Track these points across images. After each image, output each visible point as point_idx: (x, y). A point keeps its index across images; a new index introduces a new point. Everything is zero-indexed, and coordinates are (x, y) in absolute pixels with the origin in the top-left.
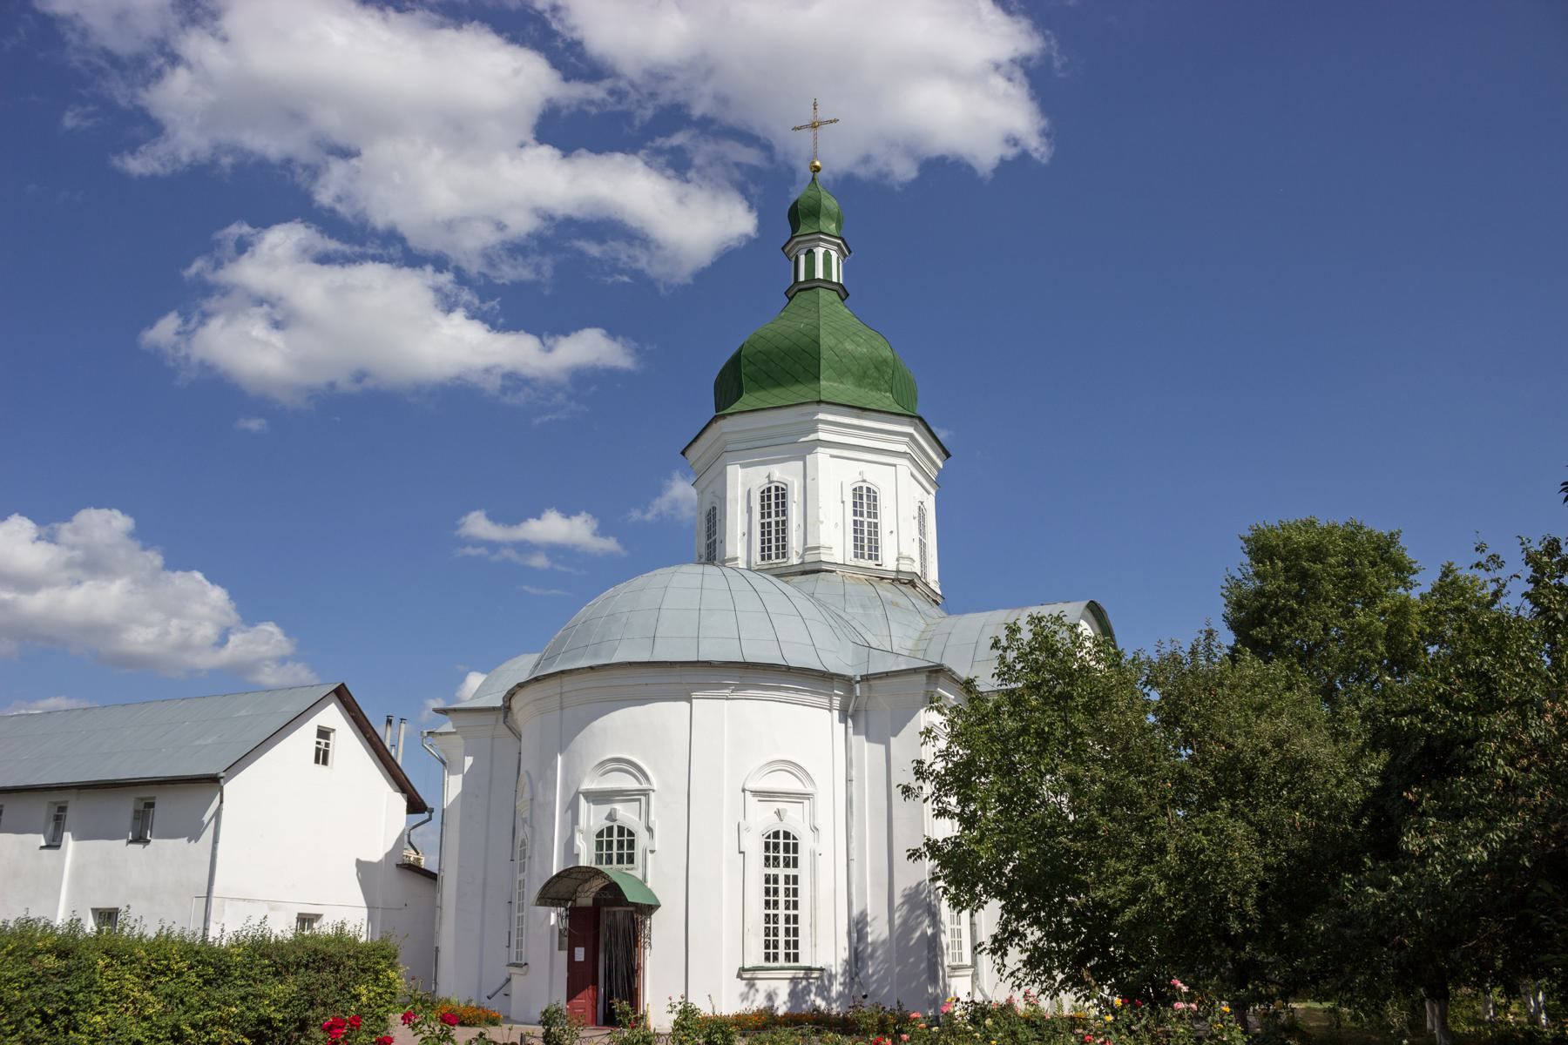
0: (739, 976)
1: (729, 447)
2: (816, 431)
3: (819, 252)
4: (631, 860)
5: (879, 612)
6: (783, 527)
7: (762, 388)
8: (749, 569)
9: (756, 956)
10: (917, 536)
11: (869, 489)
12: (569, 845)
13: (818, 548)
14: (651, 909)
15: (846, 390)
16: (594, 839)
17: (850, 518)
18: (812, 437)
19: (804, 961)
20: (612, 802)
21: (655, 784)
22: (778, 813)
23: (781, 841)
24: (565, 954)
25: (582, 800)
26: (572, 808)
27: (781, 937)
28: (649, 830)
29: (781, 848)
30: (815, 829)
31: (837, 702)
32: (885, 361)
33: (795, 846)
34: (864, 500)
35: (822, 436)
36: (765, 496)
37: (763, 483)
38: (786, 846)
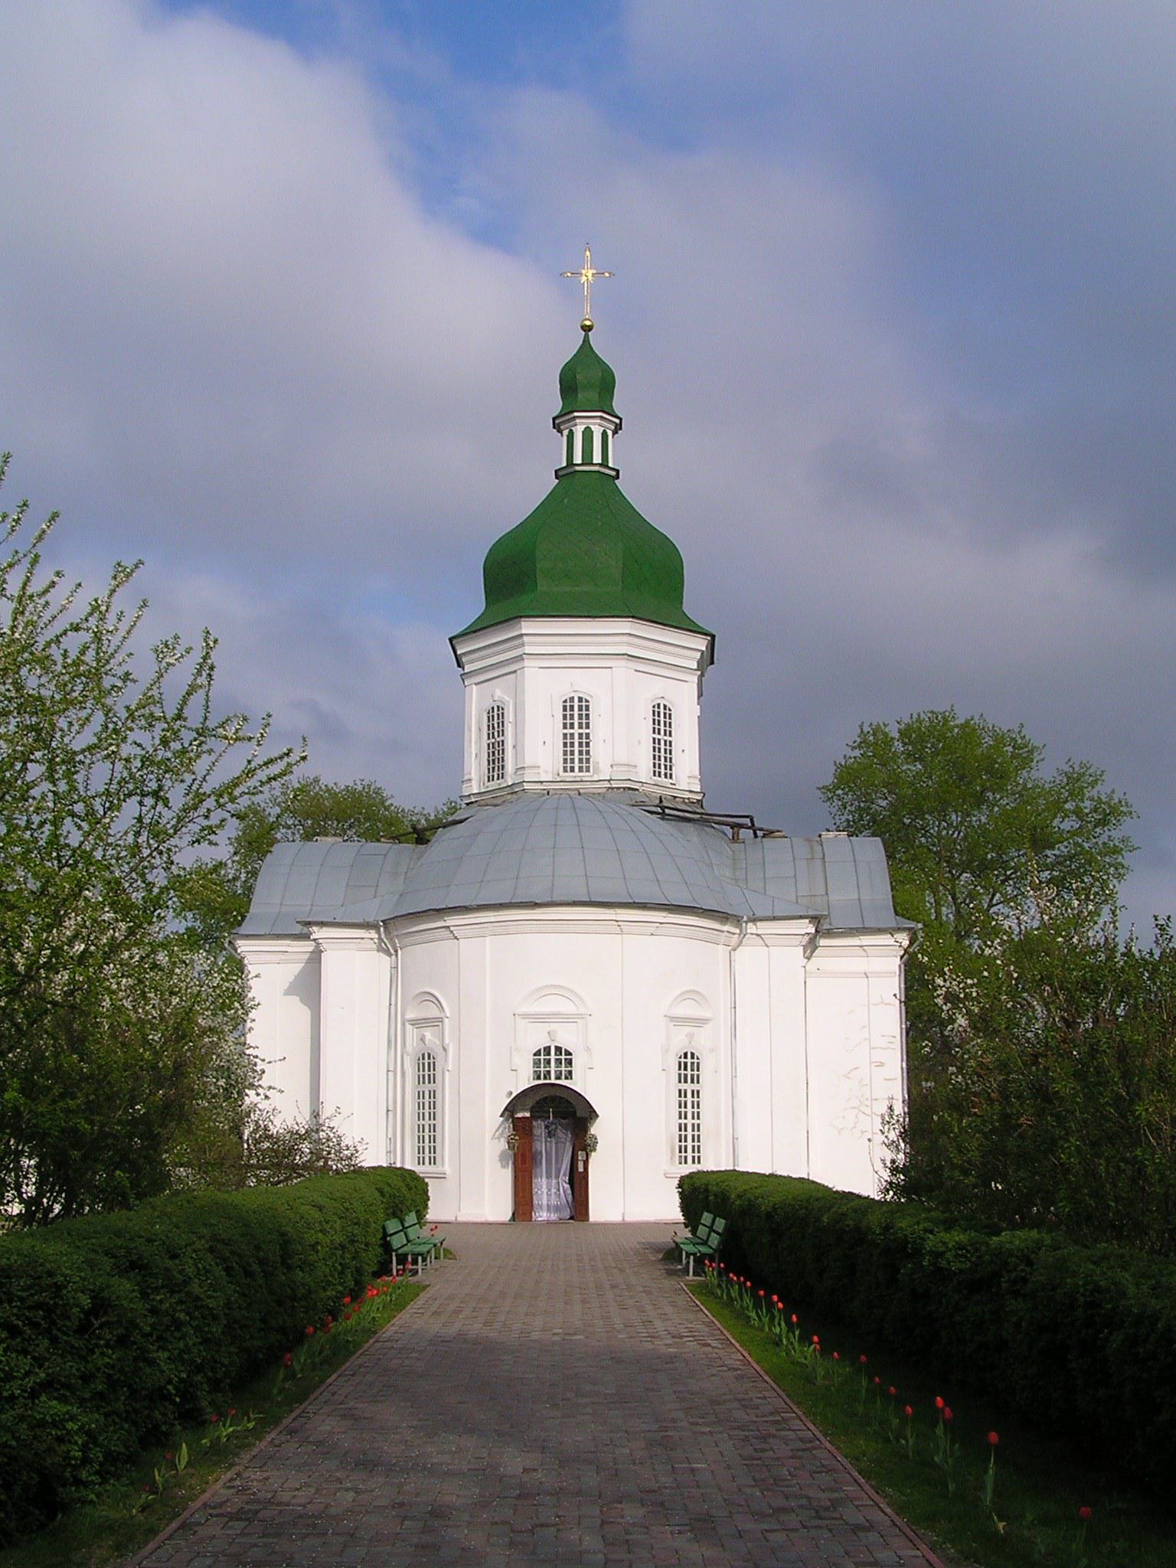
6: (586, 742)
23: (689, 1060)
28: (588, 1049)
29: (688, 1066)
36: (567, 707)
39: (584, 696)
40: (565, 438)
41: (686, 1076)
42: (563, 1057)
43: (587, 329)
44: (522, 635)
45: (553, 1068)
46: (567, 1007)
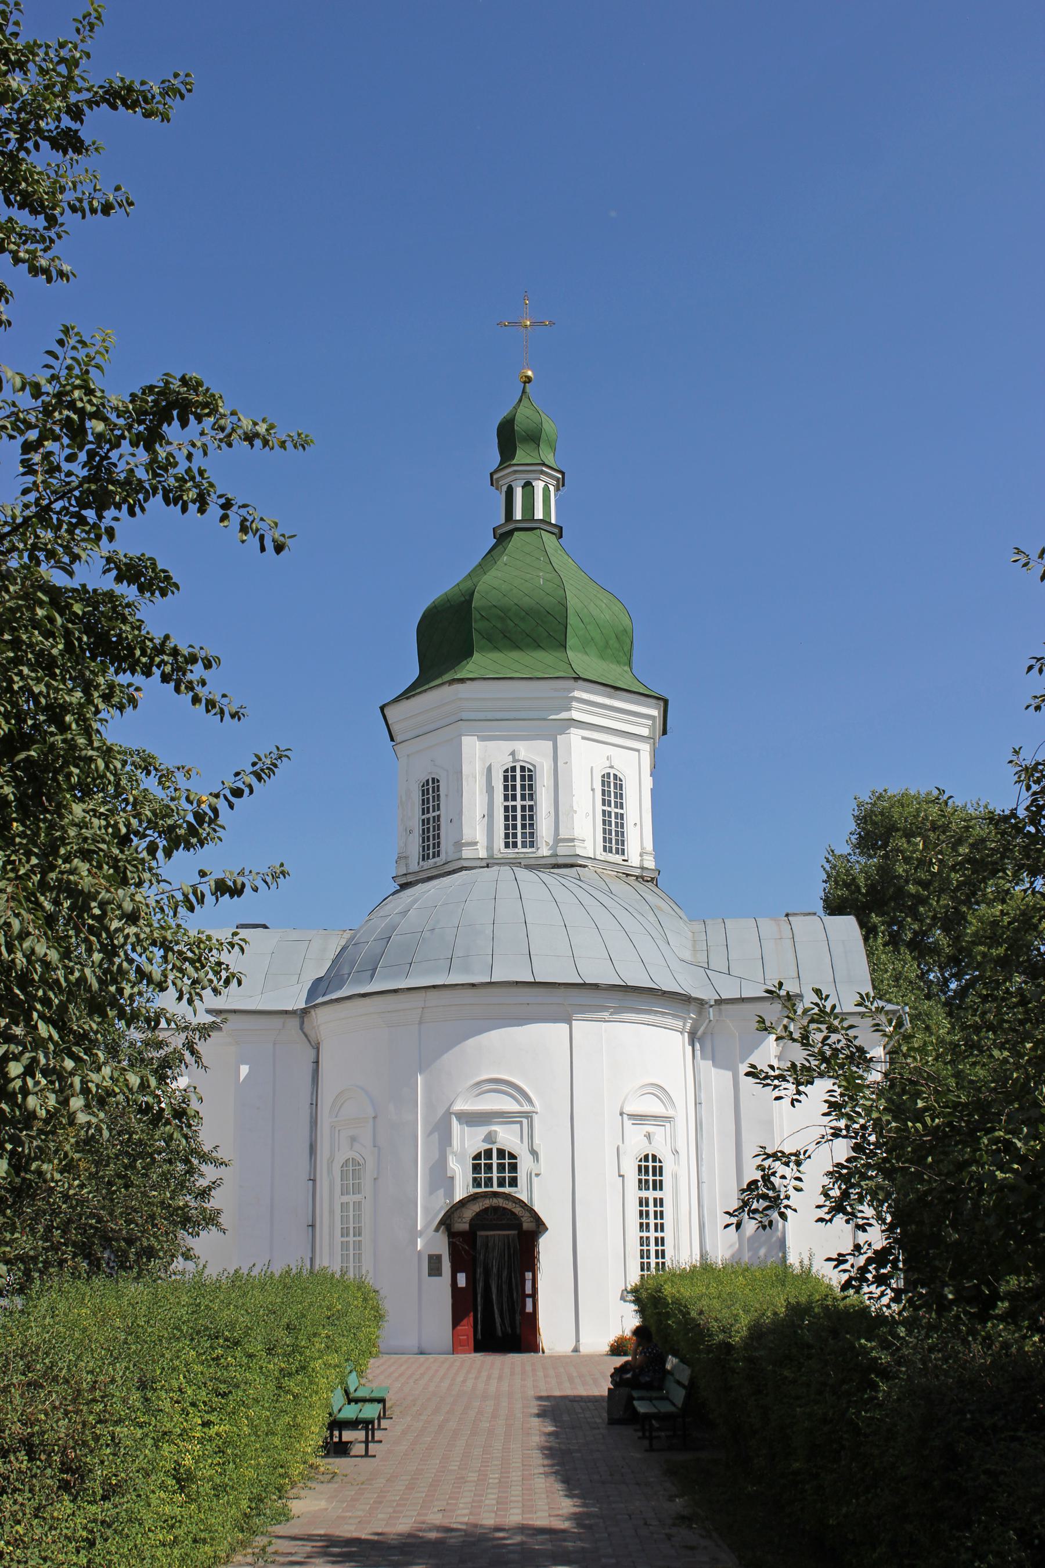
0: (623, 1298)
2: (569, 709)
3: (539, 486)
4: (514, 1182)
6: (530, 814)
7: (497, 648)
11: (615, 776)
13: (573, 840)
17: (599, 807)
18: (564, 715)
21: (538, 1106)
22: (648, 1136)
23: (650, 1164)
25: (455, 1121)
28: (534, 1153)
29: (651, 1171)
35: (575, 715)
36: (509, 776)
39: (527, 766)
40: (504, 494)
41: (647, 1181)
42: (507, 1161)
44: (461, 699)
45: (495, 1175)
46: (509, 1105)
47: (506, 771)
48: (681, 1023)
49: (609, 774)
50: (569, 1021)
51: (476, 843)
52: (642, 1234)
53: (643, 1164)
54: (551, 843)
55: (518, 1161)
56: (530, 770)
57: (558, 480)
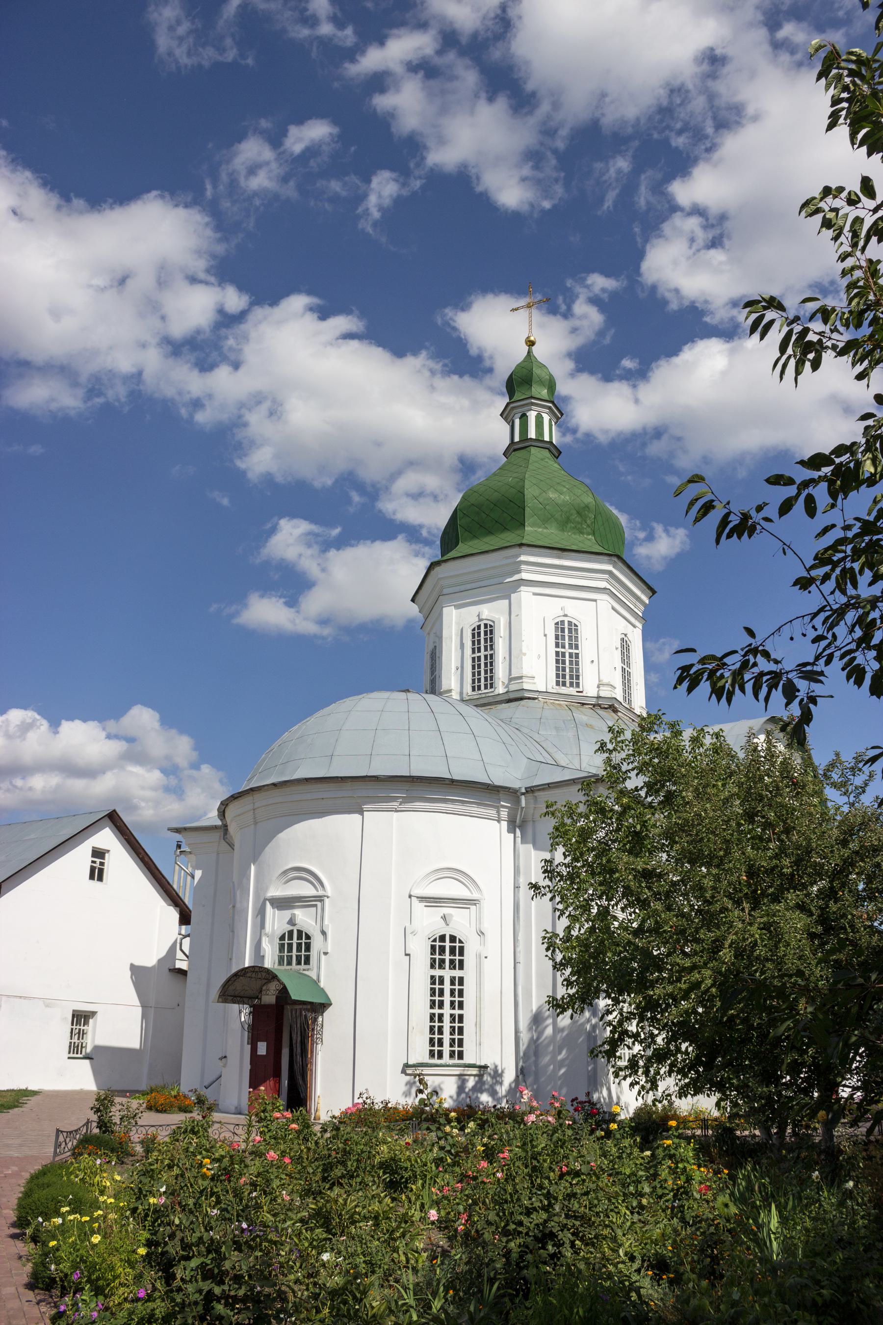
0: (403, 1072)
1: (445, 591)
2: (519, 572)
3: (532, 415)
4: (307, 961)
5: (571, 734)
6: (490, 660)
7: (475, 537)
8: (462, 700)
9: (420, 1052)
10: (619, 665)
12: (258, 946)
13: (521, 678)
14: (321, 1007)
15: (551, 534)
16: (277, 941)
17: (552, 649)
18: (516, 577)
19: (468, 1059)
20: (293, 907)
22: (444, 918)
24: (248, 1048)
26: (261, 913)
27: (446, 1034)
28: (324, 933)
29: (447, 951)
30: (481, 933)
31: (504, 813)
32: (587, 507)
33: (462, 950)
34: (566, 634)
35: (525, 576)
37: (473, 621)
38: (453, 951)
43: (531, 343)
46: (305, 889)
47: (474, 630)
48: (495, 812)
49: (563, 622)
50: (361, 812)
51: (450, 691)
52: (461, 1012)
53: (438, 944)
54: (506, 682)
55: (311, 941)
56: (491, 626)
57: (550, 408)
